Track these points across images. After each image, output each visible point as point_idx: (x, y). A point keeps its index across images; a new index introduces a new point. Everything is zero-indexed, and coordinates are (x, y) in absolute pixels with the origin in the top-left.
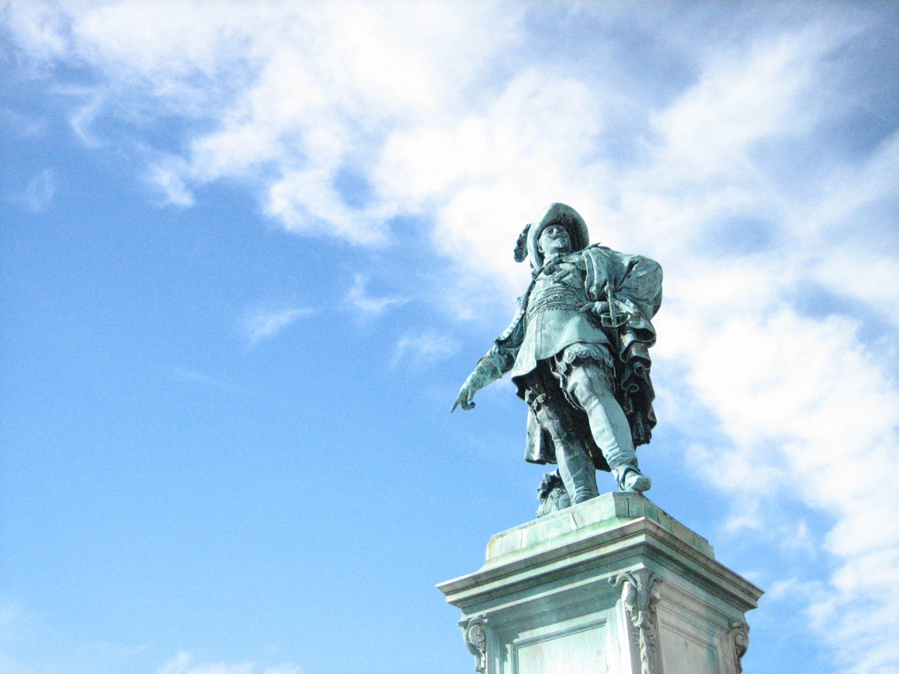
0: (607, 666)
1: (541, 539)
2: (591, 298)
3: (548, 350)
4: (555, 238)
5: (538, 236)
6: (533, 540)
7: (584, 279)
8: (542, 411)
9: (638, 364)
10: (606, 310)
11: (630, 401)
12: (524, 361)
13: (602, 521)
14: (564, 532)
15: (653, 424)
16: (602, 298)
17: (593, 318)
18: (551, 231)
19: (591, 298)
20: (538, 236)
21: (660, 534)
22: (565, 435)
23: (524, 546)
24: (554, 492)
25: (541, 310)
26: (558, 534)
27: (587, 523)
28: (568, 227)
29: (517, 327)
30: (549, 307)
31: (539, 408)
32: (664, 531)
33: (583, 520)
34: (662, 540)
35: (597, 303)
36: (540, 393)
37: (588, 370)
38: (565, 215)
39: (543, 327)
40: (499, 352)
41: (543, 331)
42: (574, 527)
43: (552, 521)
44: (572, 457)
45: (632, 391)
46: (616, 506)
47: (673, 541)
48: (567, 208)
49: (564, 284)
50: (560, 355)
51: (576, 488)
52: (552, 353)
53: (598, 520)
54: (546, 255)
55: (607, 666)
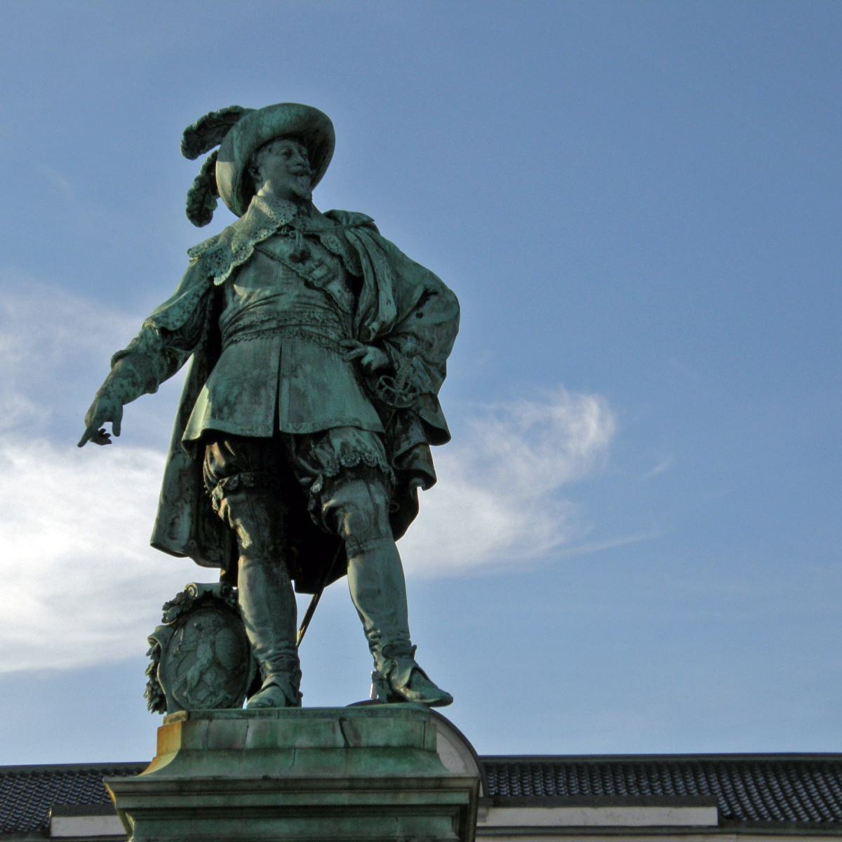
1: (280, 743)
5: (262, 145)
6: (268, 741)
10: (388, 371)
12: (238, 407)
16: (378, 343)
18: (289, 154)
19: (361, 334)
20: (262, 145)
22: (271, 548)
26: (312, 744)
29: (195, 311)
30: (304, 336)
33: (357, 736)
35: (371, 349)
37: (373, 488)
39: (294, 371)
40: (163, 351)
41: (294, 380)
42: (340, 741)
48: (327, 123)
49: (329, 297)
50: (321, 436)
51: (278, 641)
52: (306, 429)
53: (381, 743)
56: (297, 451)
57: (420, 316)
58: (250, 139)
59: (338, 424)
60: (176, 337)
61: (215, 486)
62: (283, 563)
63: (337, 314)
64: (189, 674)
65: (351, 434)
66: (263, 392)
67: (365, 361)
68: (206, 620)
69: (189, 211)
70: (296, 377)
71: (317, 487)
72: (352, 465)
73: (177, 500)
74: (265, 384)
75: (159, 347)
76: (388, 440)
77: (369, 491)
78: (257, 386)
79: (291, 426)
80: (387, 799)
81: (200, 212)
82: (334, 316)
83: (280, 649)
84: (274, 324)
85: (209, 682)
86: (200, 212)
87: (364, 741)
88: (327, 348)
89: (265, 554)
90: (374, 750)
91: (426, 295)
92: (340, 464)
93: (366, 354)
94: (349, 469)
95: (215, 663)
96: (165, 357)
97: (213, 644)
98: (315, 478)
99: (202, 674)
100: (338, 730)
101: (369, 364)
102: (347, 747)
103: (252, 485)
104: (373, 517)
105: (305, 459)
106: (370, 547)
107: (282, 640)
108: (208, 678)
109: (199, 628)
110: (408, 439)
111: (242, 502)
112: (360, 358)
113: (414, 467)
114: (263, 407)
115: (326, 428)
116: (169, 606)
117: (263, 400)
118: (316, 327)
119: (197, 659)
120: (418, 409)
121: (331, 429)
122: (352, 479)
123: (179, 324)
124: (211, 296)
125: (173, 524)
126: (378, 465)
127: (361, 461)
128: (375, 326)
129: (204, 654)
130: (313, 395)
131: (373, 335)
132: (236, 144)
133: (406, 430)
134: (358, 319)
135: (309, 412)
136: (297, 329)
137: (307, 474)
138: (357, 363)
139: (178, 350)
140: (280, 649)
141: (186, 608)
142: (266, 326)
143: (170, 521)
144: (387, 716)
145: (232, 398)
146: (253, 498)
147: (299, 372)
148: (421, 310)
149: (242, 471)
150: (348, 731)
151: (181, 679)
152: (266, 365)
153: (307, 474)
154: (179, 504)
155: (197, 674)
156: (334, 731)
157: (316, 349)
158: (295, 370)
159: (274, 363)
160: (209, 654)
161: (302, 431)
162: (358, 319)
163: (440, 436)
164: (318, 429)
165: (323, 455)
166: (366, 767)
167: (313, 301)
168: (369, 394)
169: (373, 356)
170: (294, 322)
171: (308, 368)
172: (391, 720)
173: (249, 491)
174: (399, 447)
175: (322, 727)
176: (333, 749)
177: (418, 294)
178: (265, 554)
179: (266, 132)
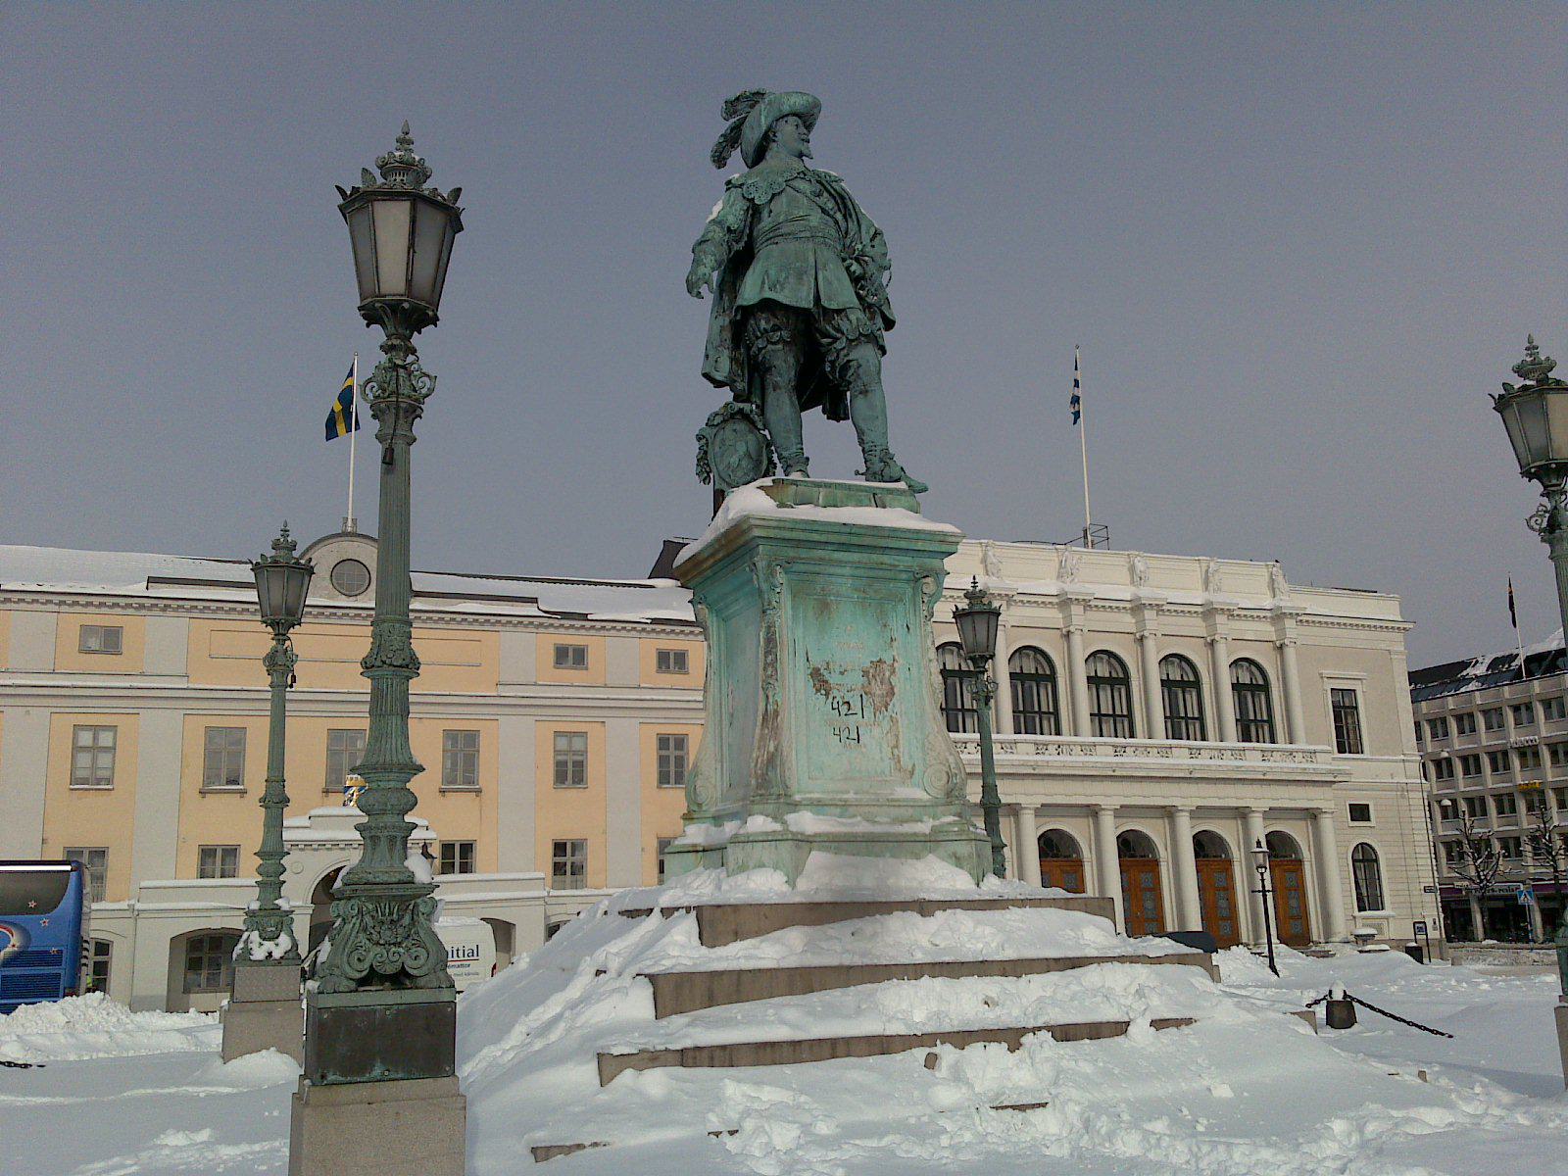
8: (780, 346)
52: (834, 306)
61: (757, 338)
66: (805, 277)
67: (853, 269)
68: (741, 426)
69: (713, 156)
71: (838, 345)
78: (800, 275)
81: (720, 160)
84: (808, 234)
86: (720, 160)
94: (865, 336)
95: (748, 455)
98: (836, 339)
101: (854, 272)
108: (744, 463)
114: (805, 288)
129: (742, 449)
132: (764, 113)
134: (848, 242)
137: (828, 336)
138: (847, 269)
141: (730, 416)
151: (726, 463)
152: (806, 260)
153: (828, 336)
160: (745, 449)
162: (848, 242)
163: (889, 324)
165: (845, 326)
173: (786, 343)
179: (786, 109)
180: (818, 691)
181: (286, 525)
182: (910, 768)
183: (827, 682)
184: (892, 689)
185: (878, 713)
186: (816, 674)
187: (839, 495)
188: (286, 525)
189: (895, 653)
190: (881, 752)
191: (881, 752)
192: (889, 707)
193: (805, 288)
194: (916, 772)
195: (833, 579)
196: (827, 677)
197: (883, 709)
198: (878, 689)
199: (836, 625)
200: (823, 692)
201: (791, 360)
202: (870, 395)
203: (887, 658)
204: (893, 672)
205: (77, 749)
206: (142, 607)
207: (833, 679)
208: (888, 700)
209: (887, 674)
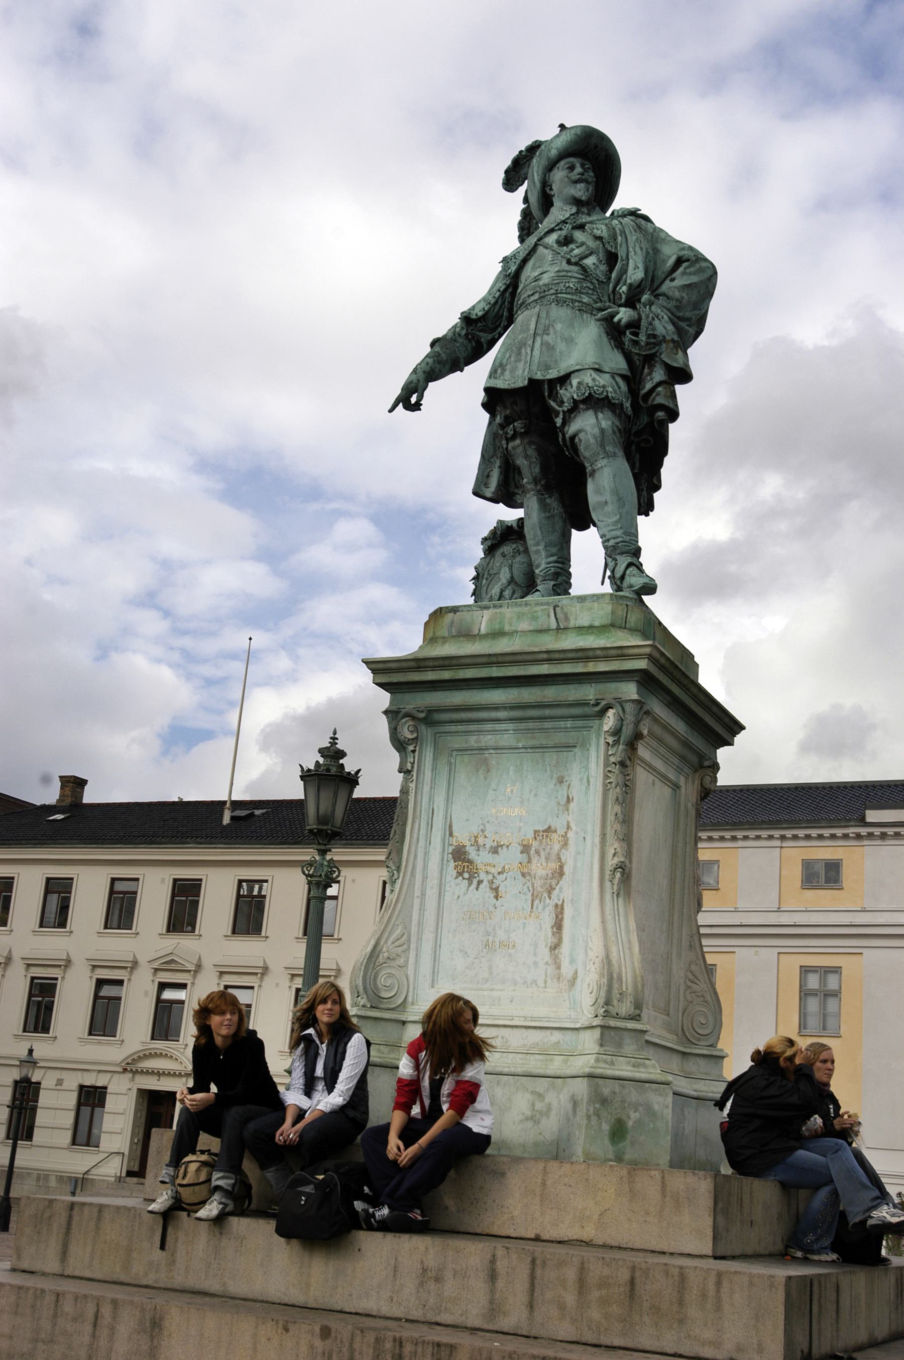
0: (568, 797)
1: (507, 628)
2: (614, 298)
3: (547, 368)
4: (576, 182)
5: (551, 166)
6: (497, 627)
7: (611, 270)
8: (518, 442)
9: (660, 414)
10: (634, 325)
11: (638, 457)
12: (508, 367)
13: (591, 627)
14: (540, 628)
15: (658, 487)
17: (615, 333)
18: (572, 168)
19: (614, 298)
20: (551, 166)
21: (663, 661)
22: (543, 482)
23: (483, 631)
24: (507, 549)
25: (545, 301)
26: (531, 628)
27: (572, 625)
28: (593, 159)
29: (496, 302)
30: (558, 302)
31: (513, 438)
32: (668, 659)
33: (567, 618)
34: (661, 667)
35: (623, 309)
36: (520, 419)
37: (600, 415)
38: (596, 147)
39: (546, 331)
40: (467, 335)
41: (546, 337)
42: (554, 625)
43: (526, 609)
44: (548, 514)
45: (642, 445)
46: (613, 613)
47: (672, 669)
49: (584, 269)
50: (564, 379)
51: (547, 557)
52: (553, 374)
53: (586, 624)
54: (557, 203)
55: (568, 797)
56: (550, 396)
57: (673, 280)
58: (544, 162)
59: (578, 367)
60: (479, 324)
62: (556, 495)
63: (592, 283)
64: (494, 592)
65: (588, 374)
66: (523, 351)
70: (548, 334)
72: (581, 398)
73: (492, 457)
74: (525, 345)
75: (464, 332)
76: (633, 379)
77: (597, 418)
79: (539, 373)
80: (579, 668)
82: (589, 285)
83: (549, 563)
84: (536, 296)
85: (507, 597)
87: (572, 624)
88: (580, 310)
89: (539, 487)
90: (580, 630)
91: (679, 262)
92: (573, 398)
93: (618, 313)
95: (512, 581)
96: (470, 340)
97: (511, 567)
99: (502, 591)
100: (552, 615)
101: (620, 320)
102: (558, 629)
103: (523, 430)
104: (599, 439)
105: (554, 401)
106: (599, 465)
107: (551, 556)
108: (507, 593)
109: (503, 555)
110: (652, 379)
111: (519, 446)
112: (613, 316)
113: (655, 402)
114: (522, 362)
115: (568, 372)
116: (485, 540)
117: (523, 358)
118: (572, 294)
119: (500, 579)
120: (661, 354)
121: (573, 372)
122: (584, 410)
123: (480, 314)
124: (510, 290)
125: (488, 476)
126: (607, 396)
127: (590, 394)
128: (624, 288)
130: (561, 346)
131: (624, 296)
133: (650, 373)
135: (556, 361)
136: (553, 297)
139: (481, 334)
140: (549, 563)
142: (532, 298)
143: (486, 474)
144: (594, 601)
145: (504, 361)
146: (526, 441)
147: (551, 329)
148: (674, 275)
149: (516, 421)
150: (560, 615)
151: (489, 596)
154: (492, 460)
155: (498, 591)
156: (549, 616)
157: (569, 312)
158: (548, 329)
159: (533, 326)
160: (508, 576)
161: (548, 377)
164: (562, 373)
166: (570, 642)
167: (569, 274)
168: (619, 345)
169: (624, 315)
170: (552, 291)
171: (559, 326)
172: (596, 605)
173: (523, 435)
174: (644, 387)
175: (540, 614)
176: (547, 631)
177: (671, 262)
178: (539, 487)
180: (460, 874)
181: (335, 733)
182: (570, 975)
183: (470, 862)
184: (561, 867)
185: (537, 902)
186: (459, 854)
187: (508, 615)
188: (335, 733)
189: (570, 819)
190: (535, 954)
191: (535, 954)
192: (555, 893)
193: (522, 362)
194: (579, 981)
195: (489, 726)
196: (472, 853)
197: (546, 895)
198: (540, 868)
199: (493, 785)
200: (466, 875)
201: (531, 451)
202: (597, 475)
203: (559, 824)
204: (565, 844)
205: (805, 994)
206: (883, 836)
207: (481, 858)
208: (554, 883)
209: (557, 847)
